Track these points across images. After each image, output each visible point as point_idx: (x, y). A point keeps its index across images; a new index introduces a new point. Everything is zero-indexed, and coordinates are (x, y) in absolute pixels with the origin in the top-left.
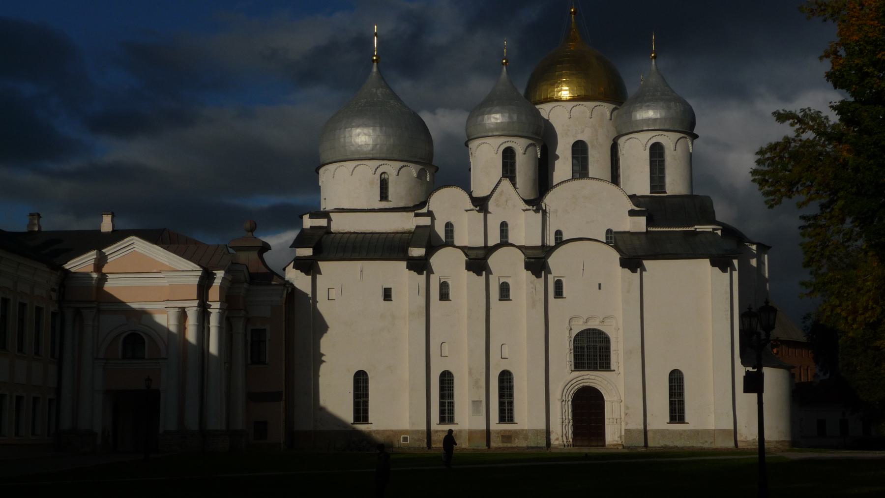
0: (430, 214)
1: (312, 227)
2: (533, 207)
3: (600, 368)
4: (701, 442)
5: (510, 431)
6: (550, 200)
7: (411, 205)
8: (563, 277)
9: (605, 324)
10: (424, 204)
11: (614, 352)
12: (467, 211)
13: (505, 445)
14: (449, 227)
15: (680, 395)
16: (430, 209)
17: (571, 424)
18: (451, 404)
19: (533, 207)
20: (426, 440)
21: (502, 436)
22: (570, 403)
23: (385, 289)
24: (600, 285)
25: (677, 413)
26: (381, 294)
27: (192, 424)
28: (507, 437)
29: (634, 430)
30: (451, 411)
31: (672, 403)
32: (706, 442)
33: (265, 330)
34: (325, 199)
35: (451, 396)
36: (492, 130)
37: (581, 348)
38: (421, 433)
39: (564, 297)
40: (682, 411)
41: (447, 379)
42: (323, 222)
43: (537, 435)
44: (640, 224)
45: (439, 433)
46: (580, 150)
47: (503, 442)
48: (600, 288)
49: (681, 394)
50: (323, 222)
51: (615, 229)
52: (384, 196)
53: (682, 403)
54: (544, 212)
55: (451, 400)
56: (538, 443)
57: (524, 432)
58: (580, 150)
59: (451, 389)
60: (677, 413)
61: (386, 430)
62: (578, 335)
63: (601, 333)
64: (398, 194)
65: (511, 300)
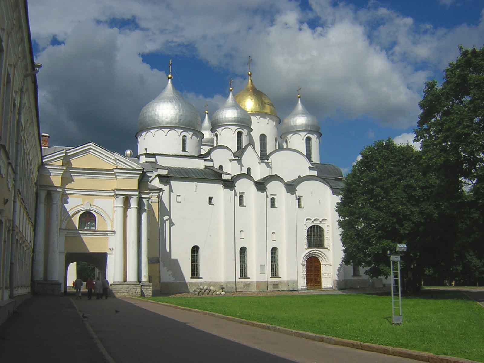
0: (211, 160)
3: (320, 247)
6: (273, 159)
8: (302, 197)
9: (322, 223)
11: (327, 238)
12: (230, 160)
13: (275, 290)
14: (221, 167)
16: (211, 158)
21: (274, 284)
23: (209, 197)
27: (132, 277)
28: (276, 285)
34: (146, 149)
36: (232, 121)
39: (302, 207)
41: (243, 251)
42: (153, 160)
43: (294, 284)
47: (274, 288)
50: (153, 160)
52: (184, 149)
58: (263, 137)
62: (309, 229)
63: (320, 227)
64: (191, 149)
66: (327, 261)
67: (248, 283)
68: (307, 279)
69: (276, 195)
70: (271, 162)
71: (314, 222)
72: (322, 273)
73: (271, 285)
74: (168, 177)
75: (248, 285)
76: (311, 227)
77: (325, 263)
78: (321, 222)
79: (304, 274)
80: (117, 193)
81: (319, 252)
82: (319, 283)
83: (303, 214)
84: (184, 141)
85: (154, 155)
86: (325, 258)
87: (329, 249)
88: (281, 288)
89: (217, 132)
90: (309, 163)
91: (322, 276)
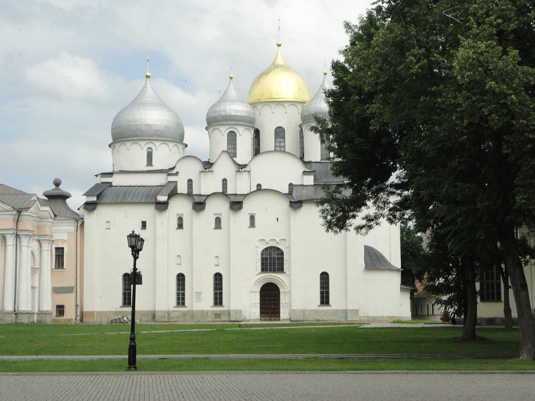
1: (102, 183)
2: (242, 169)
4: (339, 317)
5: (219, 311)
8: (255, 214)
11: (287, 261)
12: (201, 172)
13: (217, 320)
14: (190, 181)
15: (327, 288)
17: (259, 306)
18: (183, 294)
20: (166, 317)
21: (215, 314)
22: (259, 293)
24: (277, 219)
25: (325, 299)
28: (218, 315)
29: (297, 310)
30: (183, 299)
31: (322, 293)
32: (342, 317)
33: (63, 248)
35: (184, 289)
37: (266, 258)
38: (163, 312)
40: (328, 298)
44: (309, 180)
45: (175, 312)
46: (280, 132)
48: (277, 220)
49: (328, 288)
51: (294, 184)
53: (328, 293)
54: (249, 172)
55: (183, 292)
56: (236, 318)
57: (229, 311)
58: (280, 132)
59: (184, 285)
60: (325, 299)
61: (143, 311)
62: (263, 250)
63: (278, 249)
66: (285, 288)
67: (185, 312)
68: (261, 309)
69: (221, 214)
71: (270, 243)
72: (281, 302)
73: (212, 314)
75: (185, 314)
76: (266, 249)
77: (284, 291)
78: (278, 242)
79: (256, 302)
81: (275, 278)
82: (278, 313)
83: (256, 234)
84: (150, 156)
85: (111, 174)
86: (283, 285)
87: (287, 273)
88: (224, 318)
91: (281, 306)
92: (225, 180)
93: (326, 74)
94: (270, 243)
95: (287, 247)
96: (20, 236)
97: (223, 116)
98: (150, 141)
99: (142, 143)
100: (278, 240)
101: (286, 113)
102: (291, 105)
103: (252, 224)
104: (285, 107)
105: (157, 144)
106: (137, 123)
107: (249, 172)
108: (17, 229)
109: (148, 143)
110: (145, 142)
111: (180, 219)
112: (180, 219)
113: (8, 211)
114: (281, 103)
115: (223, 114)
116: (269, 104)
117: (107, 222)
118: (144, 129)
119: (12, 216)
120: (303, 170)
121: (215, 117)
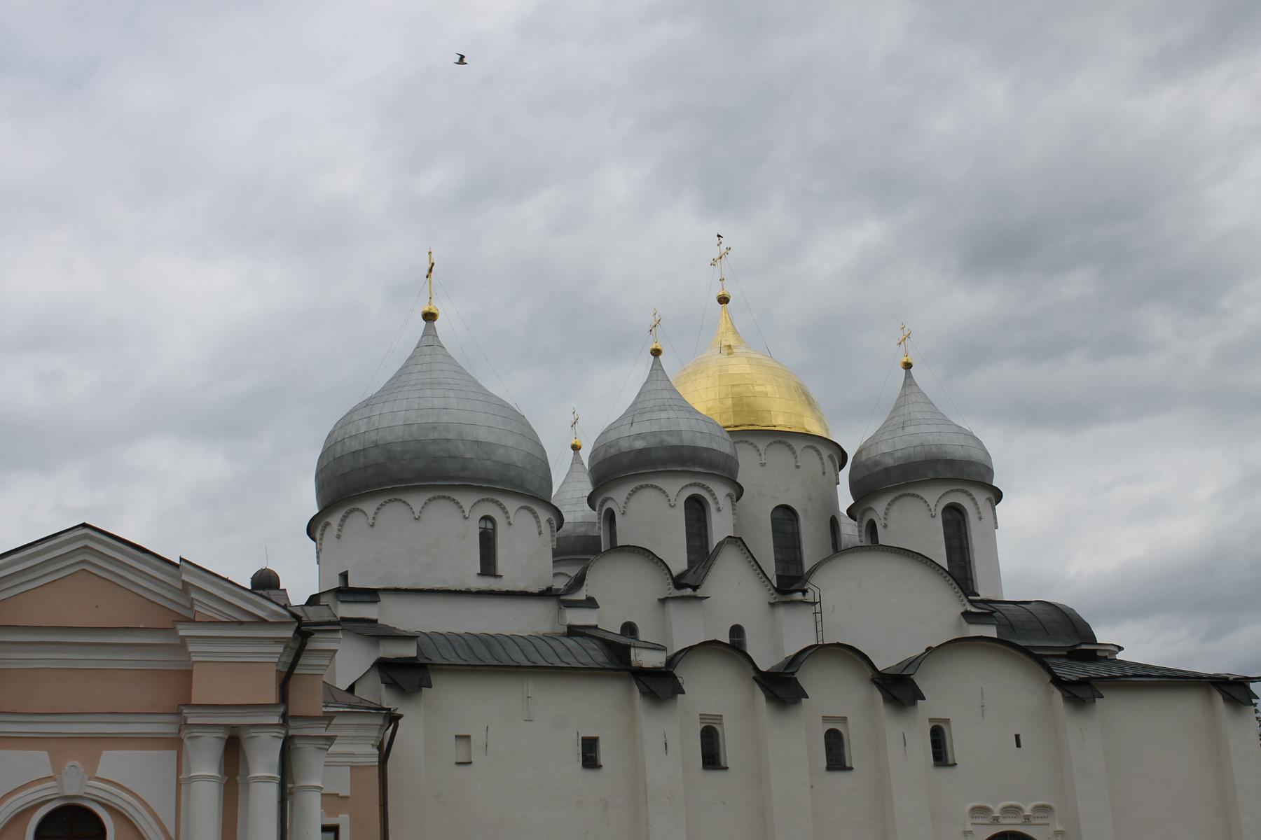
2: (804, 594)
7: (535, 590)
8: (947, 721)
10: (579, 582)
12: (663, 601)
19: (804, 594)
23: (584, 740)
24: (1017, 737)
26: (575, 753)
46: (785, 518)
48: (1018, 745)
52: (488, 565)
58: (785, 518)
65: (851, 769)
69: (844, 720)
70: (817, 600)
71: (1002, 821)
74: (424, 666)
78: (1027, 818)
80: (190, 721)
84: (488, 542)
85: (370, 595)
89: (608, 505)
90: (965, 601)
92: (737, 631)
93: (911, 367)
94: (1002, 821)
95: (1057, 833)
96: (299, 743)
97: (673, 447)
98: (490, 496)
99: (467, 500)
100: (1028, 811)
101: (798, 467)
102: (808, 447)
103: (940, 754)
104: (794, 453)
105: (512, 505)
106: (445, 435)
107: (814, 604)
108: (285, 716)
109: (483, 500)
110: (476, 497)
111: (710, 736)
112: (710, 736)
113: (262, 622)
114: (783, 439)
115: (674, 441)
116: (751, 440)
117: (456, 736)
118: (468, 456)
119: (280, 649)
120: (963, 611)
121: (640, 451)
